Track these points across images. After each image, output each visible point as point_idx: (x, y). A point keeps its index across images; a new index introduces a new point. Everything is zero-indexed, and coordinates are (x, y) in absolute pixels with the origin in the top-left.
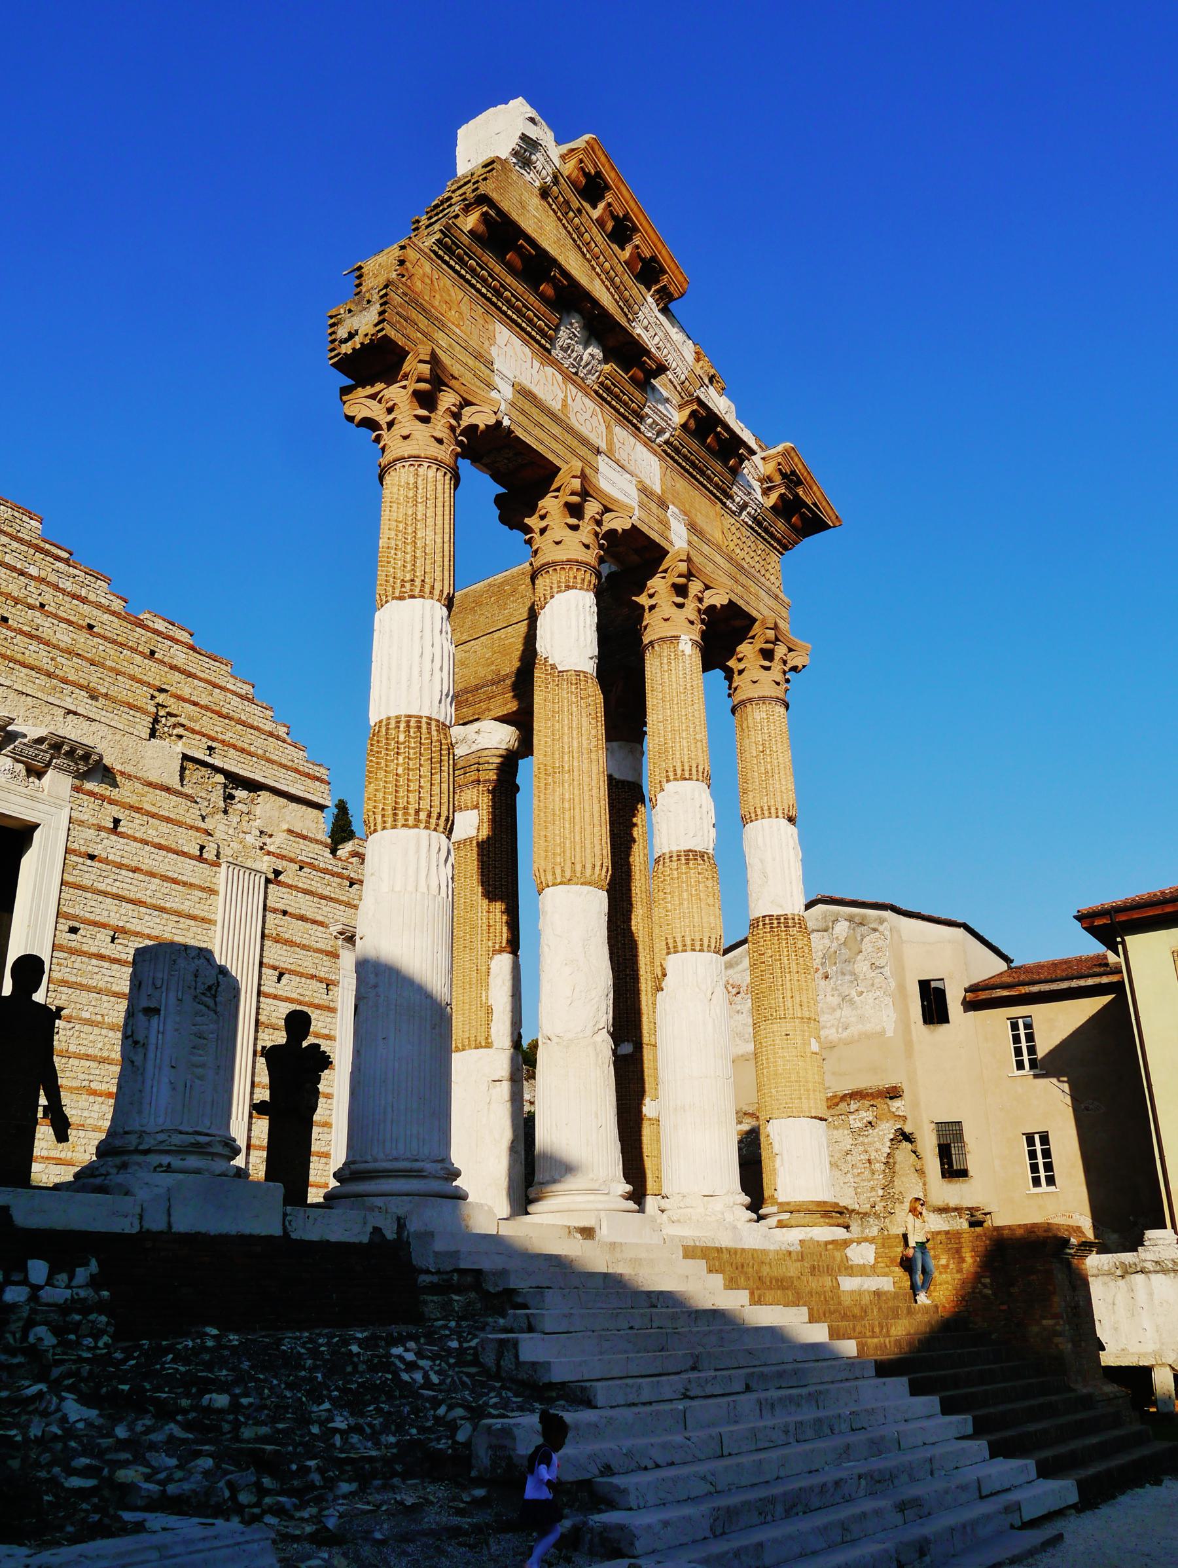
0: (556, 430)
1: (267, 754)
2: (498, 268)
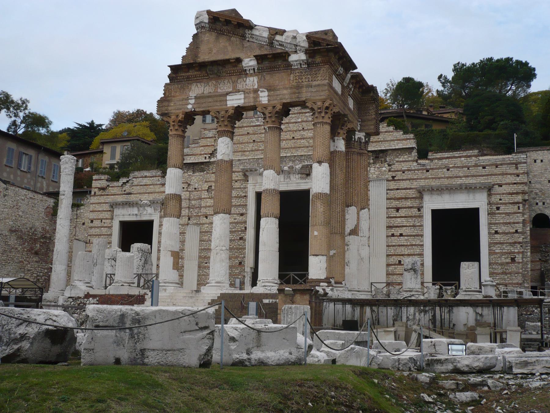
0: (210, 100)
1: (385, 139)
2: (184, 74)
